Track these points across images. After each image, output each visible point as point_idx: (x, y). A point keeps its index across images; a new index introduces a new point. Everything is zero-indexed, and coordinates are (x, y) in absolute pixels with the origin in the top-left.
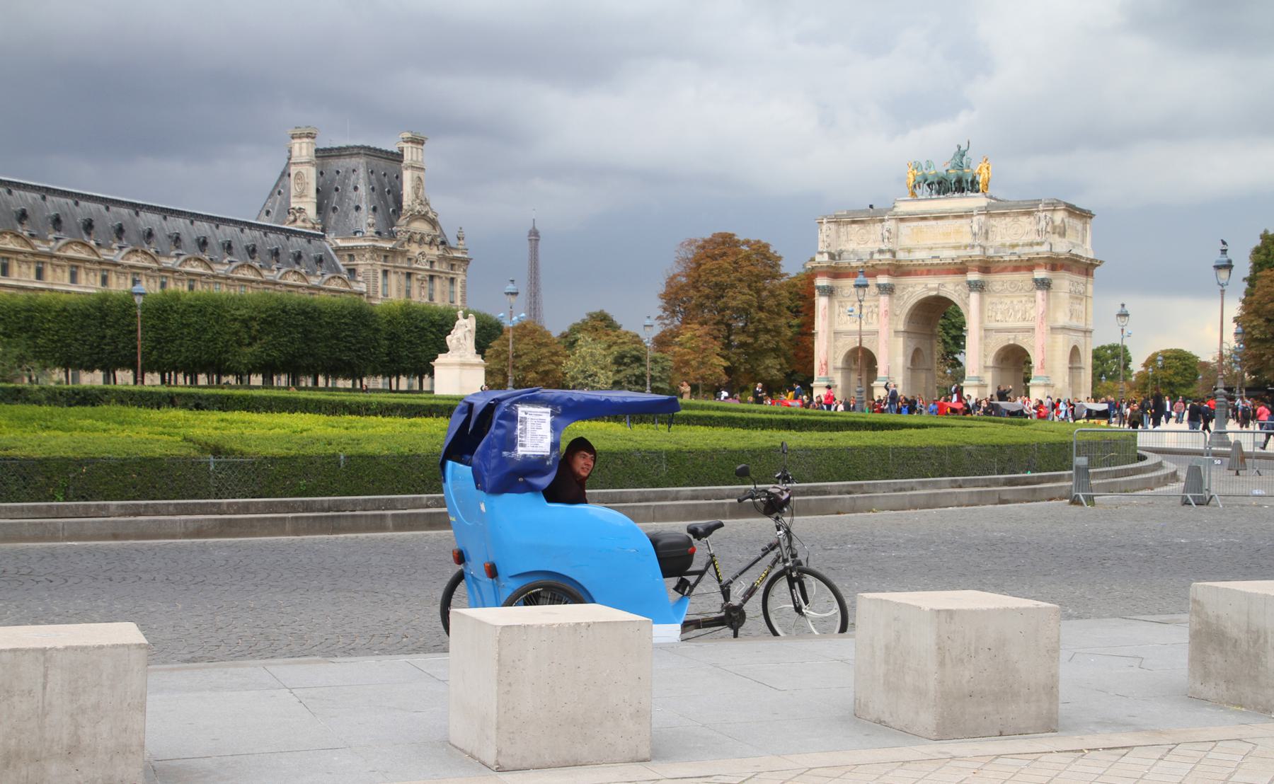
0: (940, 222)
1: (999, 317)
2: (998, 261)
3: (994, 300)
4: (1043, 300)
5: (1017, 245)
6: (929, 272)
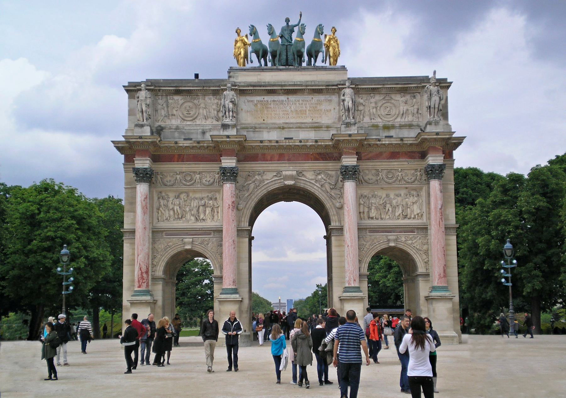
0: (292, 98)
1: (373, 213)
2: (374, 144)
3: (366, 192)
4: (441, 192)
5: (393, 127)
6: (281, 158)
